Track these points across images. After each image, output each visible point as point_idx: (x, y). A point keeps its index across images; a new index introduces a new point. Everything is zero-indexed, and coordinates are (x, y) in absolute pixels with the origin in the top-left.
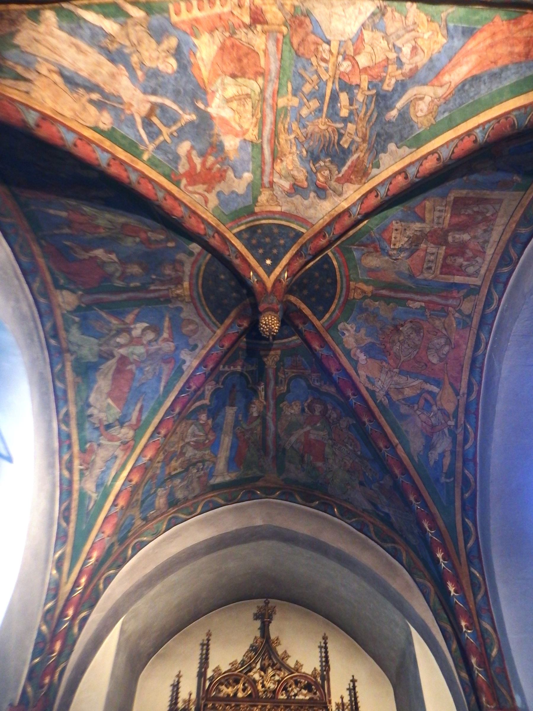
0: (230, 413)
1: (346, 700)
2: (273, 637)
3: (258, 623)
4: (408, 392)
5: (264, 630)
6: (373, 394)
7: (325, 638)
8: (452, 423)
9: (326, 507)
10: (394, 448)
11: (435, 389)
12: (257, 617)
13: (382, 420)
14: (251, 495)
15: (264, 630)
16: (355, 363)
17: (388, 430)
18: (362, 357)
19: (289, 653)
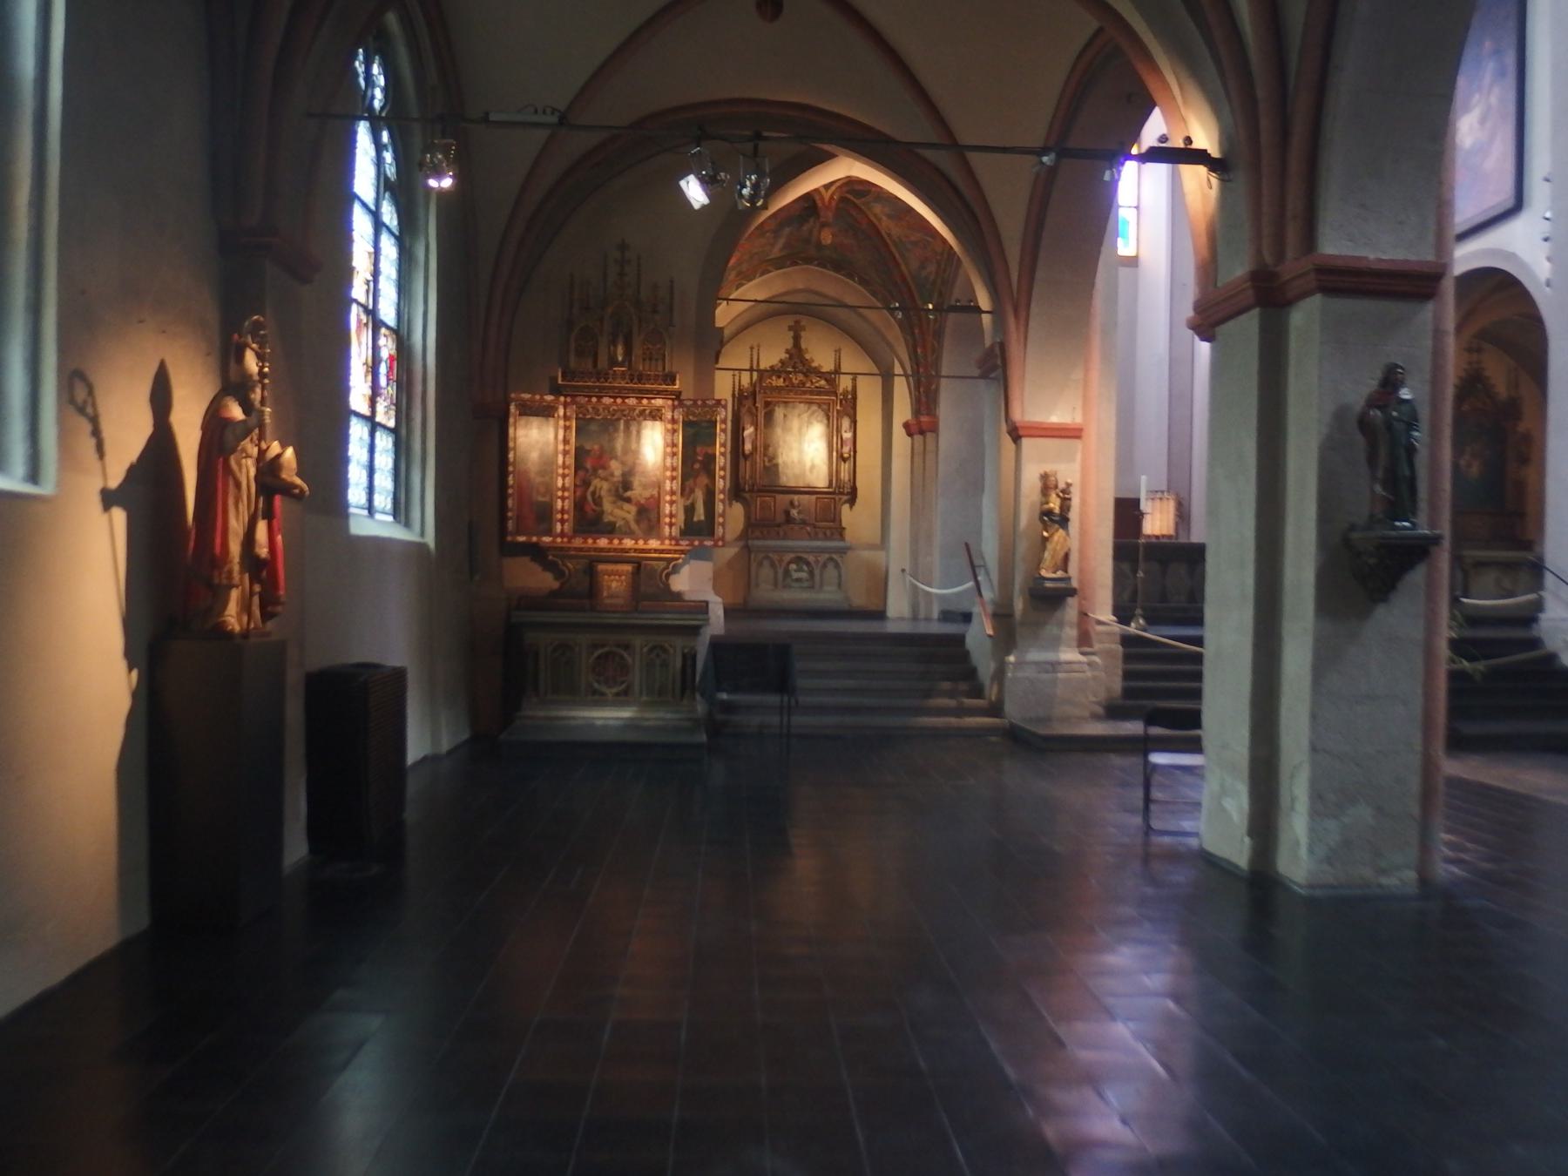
0: (787, 230)
1: (850, 389)
2: (803, 346)
3: (792, 333)
4: (913, 238)
5: (797, 339)
6: (889, 235)
7: (838, 352)
8: (938, 257)
9: (850, 276)
10: (897, 264)
11: (930, 239)
12: (790, 328)
13: (894, 250)
14: (794, 263)
15: (797, 339)
16: (880, 220)
17: (897, 256)
18: (884, 218)
19: (814, 358)
